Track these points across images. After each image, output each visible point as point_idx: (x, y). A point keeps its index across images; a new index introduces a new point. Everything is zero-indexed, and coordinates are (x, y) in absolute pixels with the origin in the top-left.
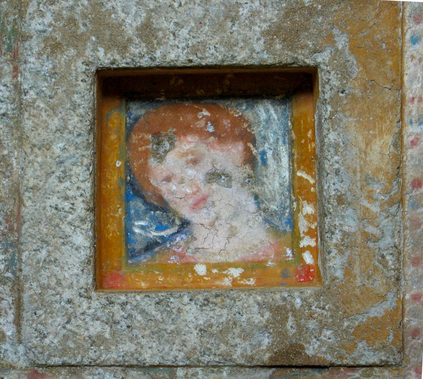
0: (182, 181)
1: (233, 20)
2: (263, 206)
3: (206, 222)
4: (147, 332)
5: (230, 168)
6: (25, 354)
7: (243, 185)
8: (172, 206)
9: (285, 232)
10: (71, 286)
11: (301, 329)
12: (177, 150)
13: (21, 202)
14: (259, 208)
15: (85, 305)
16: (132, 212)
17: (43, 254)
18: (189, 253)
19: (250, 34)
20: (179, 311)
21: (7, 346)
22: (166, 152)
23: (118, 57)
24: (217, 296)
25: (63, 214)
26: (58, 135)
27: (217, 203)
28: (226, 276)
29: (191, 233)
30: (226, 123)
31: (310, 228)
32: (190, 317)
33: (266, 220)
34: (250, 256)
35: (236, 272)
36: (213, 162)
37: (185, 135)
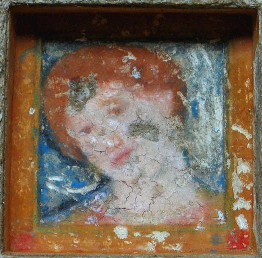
0: (103, 133)
2: (192, 163)
3: (129, 179)
5: (157, 120)
8: (91, 160)
9: (217, 192)
12: (98, 97)
14: (189, 165)
16: (46, 165)
22: (86, 100)
27: (141, 158)
28: (150, 240)
29: (112, 192)
30: (154, 69)
31: (245, 189)
33: (196, 179)
34: (177, 218)
35: (160, 236)
36: (139, 112)
37: (107, 81)
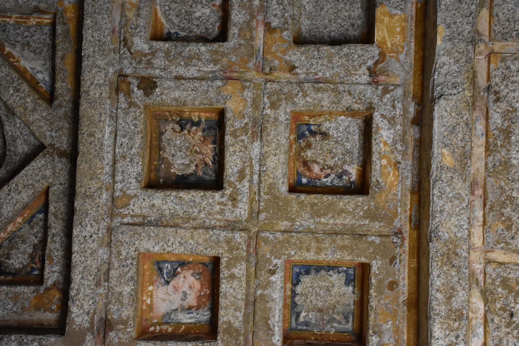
0: (184, 282)
1: (235, 310)
3: (168, 291)
4: (121, 272)
5: (187, 300)
6: (116, 226)
7: (181, 305)
8: (175, 278)
10: (140, 244)
11: (119, 330)
13: (172, 227)
15: (133, 249)
17: (152, 234)
18: (157, 283)
19: (230, 316)
20: (128, 285)
21: (120, 219)
22: (195, 277)
23: (224, 266)
24: (133, 299)
25: (167, 242)
26: (196, 242)
32: (126, 288)
33: (168, 313)
34: (155, 307)
35: (148, 301)
36: (190, 294)
